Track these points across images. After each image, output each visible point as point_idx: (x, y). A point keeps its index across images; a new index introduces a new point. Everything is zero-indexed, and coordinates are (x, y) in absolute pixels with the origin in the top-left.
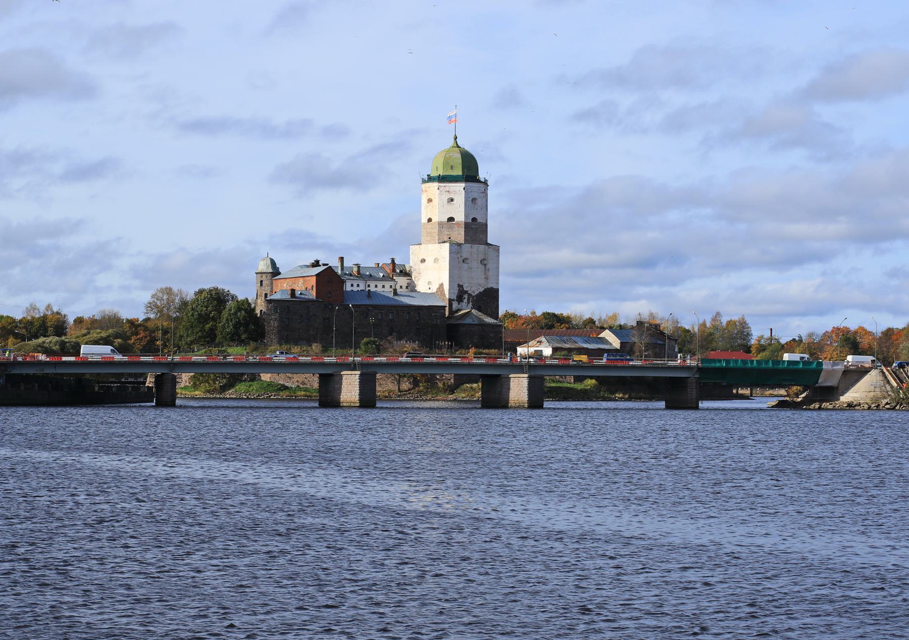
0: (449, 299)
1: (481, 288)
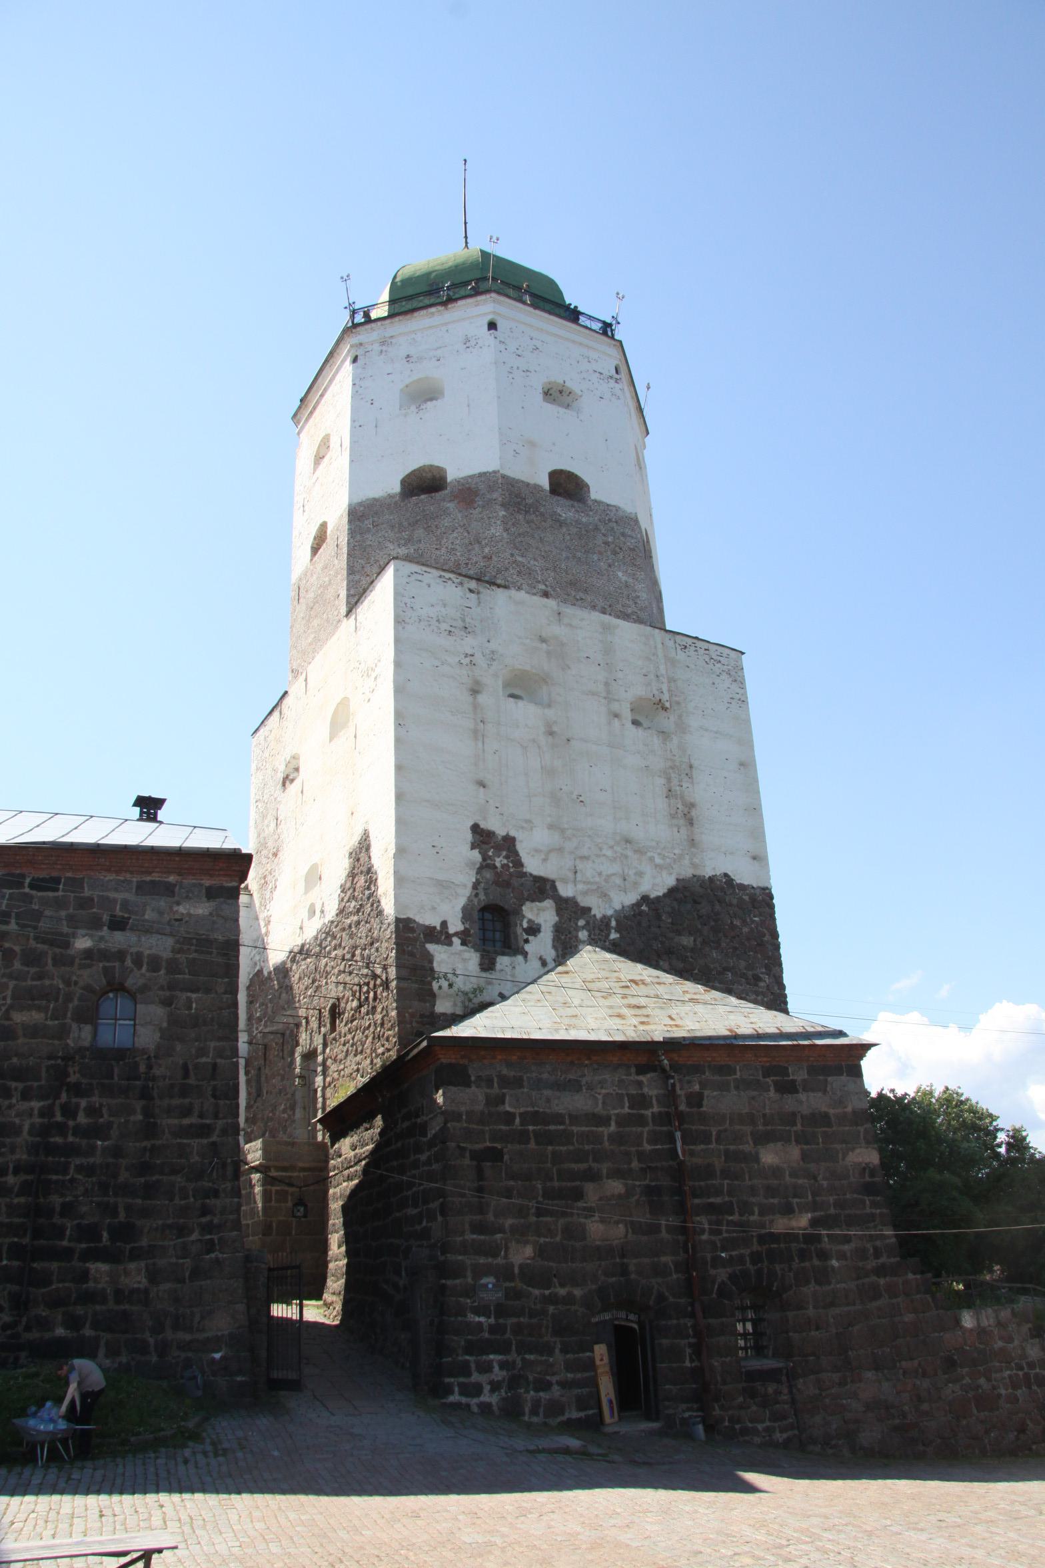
0: (398, 920)
1: (648, 869)
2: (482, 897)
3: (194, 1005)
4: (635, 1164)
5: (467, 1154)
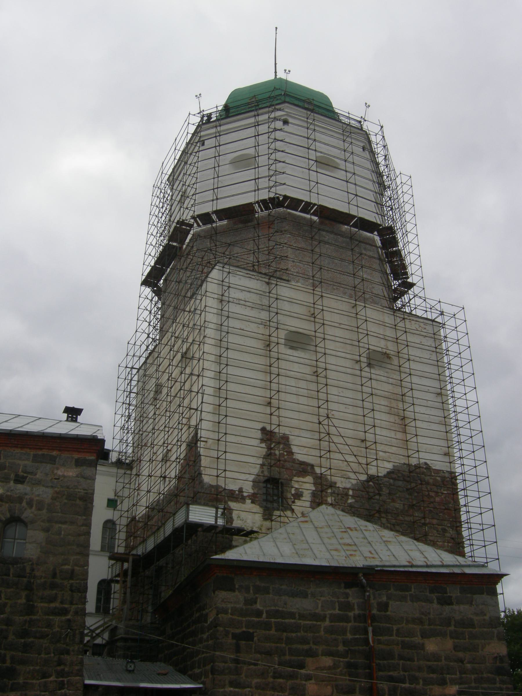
2: (266, 473)
3: (63, 533)
4: (341, 648)
5: (230, 636)
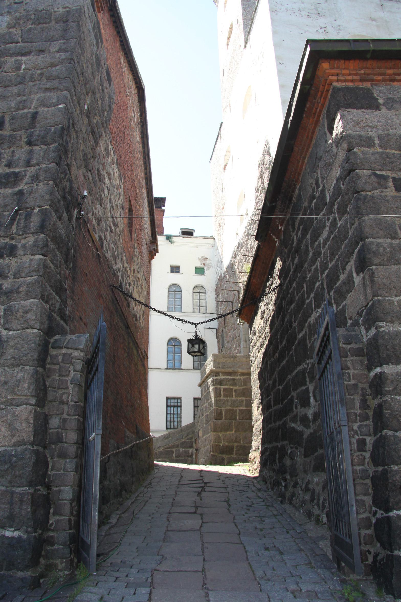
5: (390, 184)
